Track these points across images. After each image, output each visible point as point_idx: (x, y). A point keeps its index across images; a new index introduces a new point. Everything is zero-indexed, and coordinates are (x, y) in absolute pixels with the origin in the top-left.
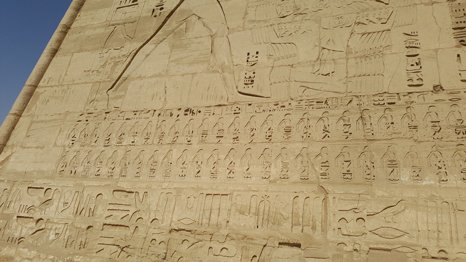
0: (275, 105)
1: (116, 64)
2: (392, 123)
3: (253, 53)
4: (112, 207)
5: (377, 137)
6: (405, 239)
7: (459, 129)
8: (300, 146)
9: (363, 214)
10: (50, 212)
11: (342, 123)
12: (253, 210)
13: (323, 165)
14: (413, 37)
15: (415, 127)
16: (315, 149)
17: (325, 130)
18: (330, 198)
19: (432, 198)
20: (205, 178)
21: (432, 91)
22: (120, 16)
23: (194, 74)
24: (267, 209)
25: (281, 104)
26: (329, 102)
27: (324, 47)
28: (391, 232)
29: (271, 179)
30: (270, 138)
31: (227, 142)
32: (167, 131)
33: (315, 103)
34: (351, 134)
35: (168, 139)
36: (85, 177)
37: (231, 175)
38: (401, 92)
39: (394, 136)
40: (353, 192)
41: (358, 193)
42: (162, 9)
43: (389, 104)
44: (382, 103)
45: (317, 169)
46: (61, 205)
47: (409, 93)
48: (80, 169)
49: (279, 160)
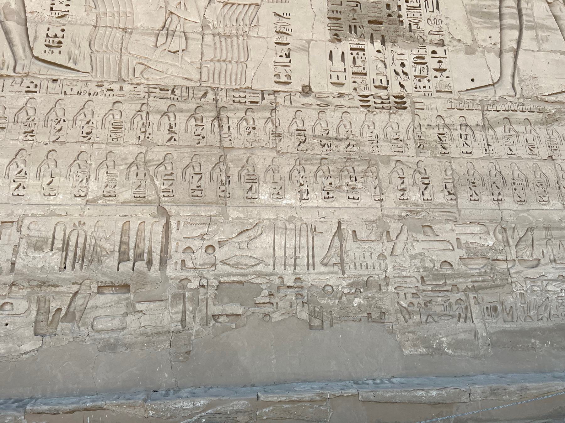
0: (98, 86)
2: (254, 128)
6: (260, 268)
7: (324, 141)
8: (135, 150)
11: (192, 122)
12: (58, 244)
13: (167, 177)
14: (284, 20)
15: (279, 135)
17: (170, 131)
21: (300, 92)
24: (81, 240)
25: (107, 86)
26: (178, 92)
29: (90, 197)
30: (89, 136)
33: (157, 90)
34: (203, 137)
37: (21, 191)
38: (267, 89)
40: (203, 214)
43: (251, 102)
44: (243, 100)
45: (157, 183)
47: (275, 92)
49: (103, 171)
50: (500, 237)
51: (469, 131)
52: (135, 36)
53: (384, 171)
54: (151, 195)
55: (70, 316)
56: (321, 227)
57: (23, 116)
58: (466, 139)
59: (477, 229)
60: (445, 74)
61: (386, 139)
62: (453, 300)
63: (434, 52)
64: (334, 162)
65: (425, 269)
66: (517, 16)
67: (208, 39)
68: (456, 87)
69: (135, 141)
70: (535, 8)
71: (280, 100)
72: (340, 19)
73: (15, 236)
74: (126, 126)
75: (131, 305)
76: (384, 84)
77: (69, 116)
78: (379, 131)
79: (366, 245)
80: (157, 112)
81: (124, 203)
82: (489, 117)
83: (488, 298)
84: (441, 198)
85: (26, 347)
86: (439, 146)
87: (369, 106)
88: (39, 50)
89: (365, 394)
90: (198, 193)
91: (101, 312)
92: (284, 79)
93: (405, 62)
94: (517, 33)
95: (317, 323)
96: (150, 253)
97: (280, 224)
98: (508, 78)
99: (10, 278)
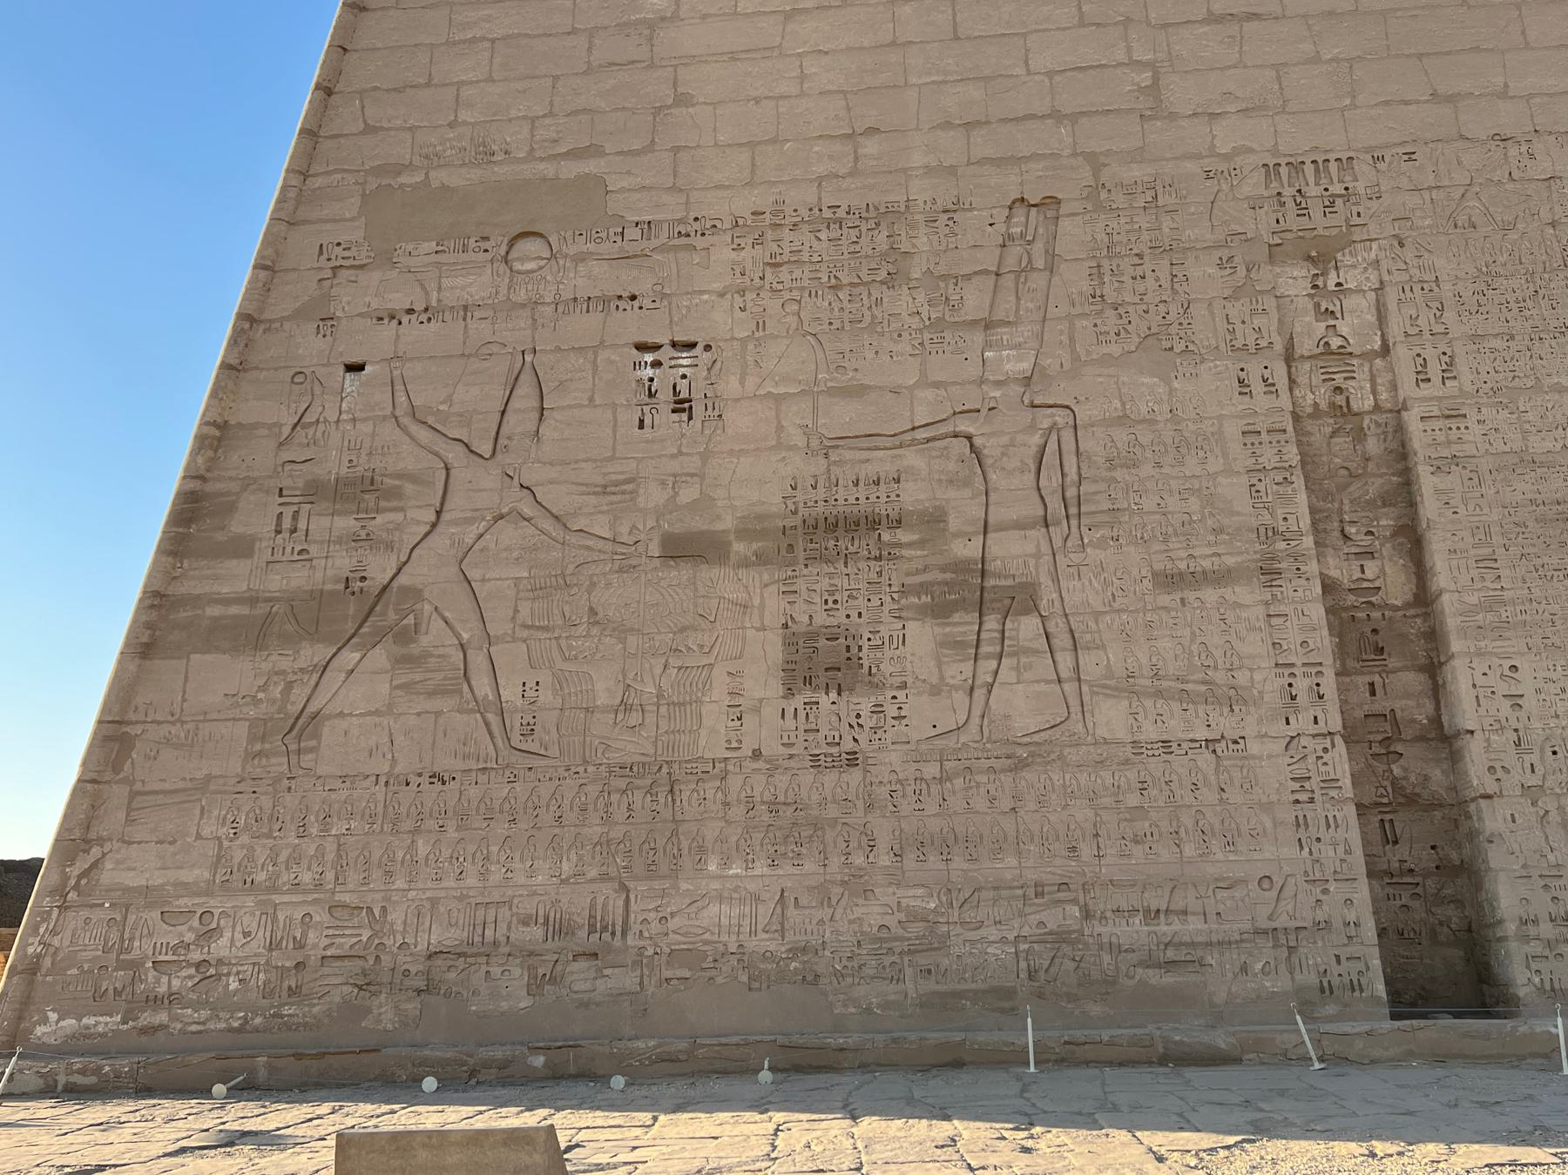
1: (289, 686)
3: (531, 684)
4: (331, 932)
6: (707, 936)
8: (599, 829)
10: (221, 947)
11: (649, 798)
12: (541, 920)
20: (471, 881)
22: (275, 583)
23: (438, 714)
25: (574, 769)
35: (408, 825)
36: (274, 889)
46: (239, 936)
48: (261, 877)
50: (944, 899)
51: (924, 786)
52: (598, 715)
53: (830, 835)
54: (613, 871)
55: (553, 980)
56: (765, 896)
57: (507, 806)
59: (920, 892)
60: (904, 722)
61: (834, 801)
62: (887, 964)
64: (780, 828)
65: (862, 933)
66: (998, 641)
67: (663, 709)
68: (915, 736)
69: (598, 821)
70: (1022, 627)
71: (730, 767)
73: (508, 914)
74: (591, 807)
75: (599, 970)
77: (543, 803)
78: (828, 793)
79: (807, 912)
80: (618, 791)
81: (592, 881)
83: (923, 960)
84: (885, 860)
85: (522, 1005)
88: (516, 740)
89: (781, 1040)
91: (576, 976)
92: (735, 745)
94: (994, 664)
95: (756, 985)
96: (613, 925)
97: (726, 894)
98: (975, 720)
99: (507, 950)
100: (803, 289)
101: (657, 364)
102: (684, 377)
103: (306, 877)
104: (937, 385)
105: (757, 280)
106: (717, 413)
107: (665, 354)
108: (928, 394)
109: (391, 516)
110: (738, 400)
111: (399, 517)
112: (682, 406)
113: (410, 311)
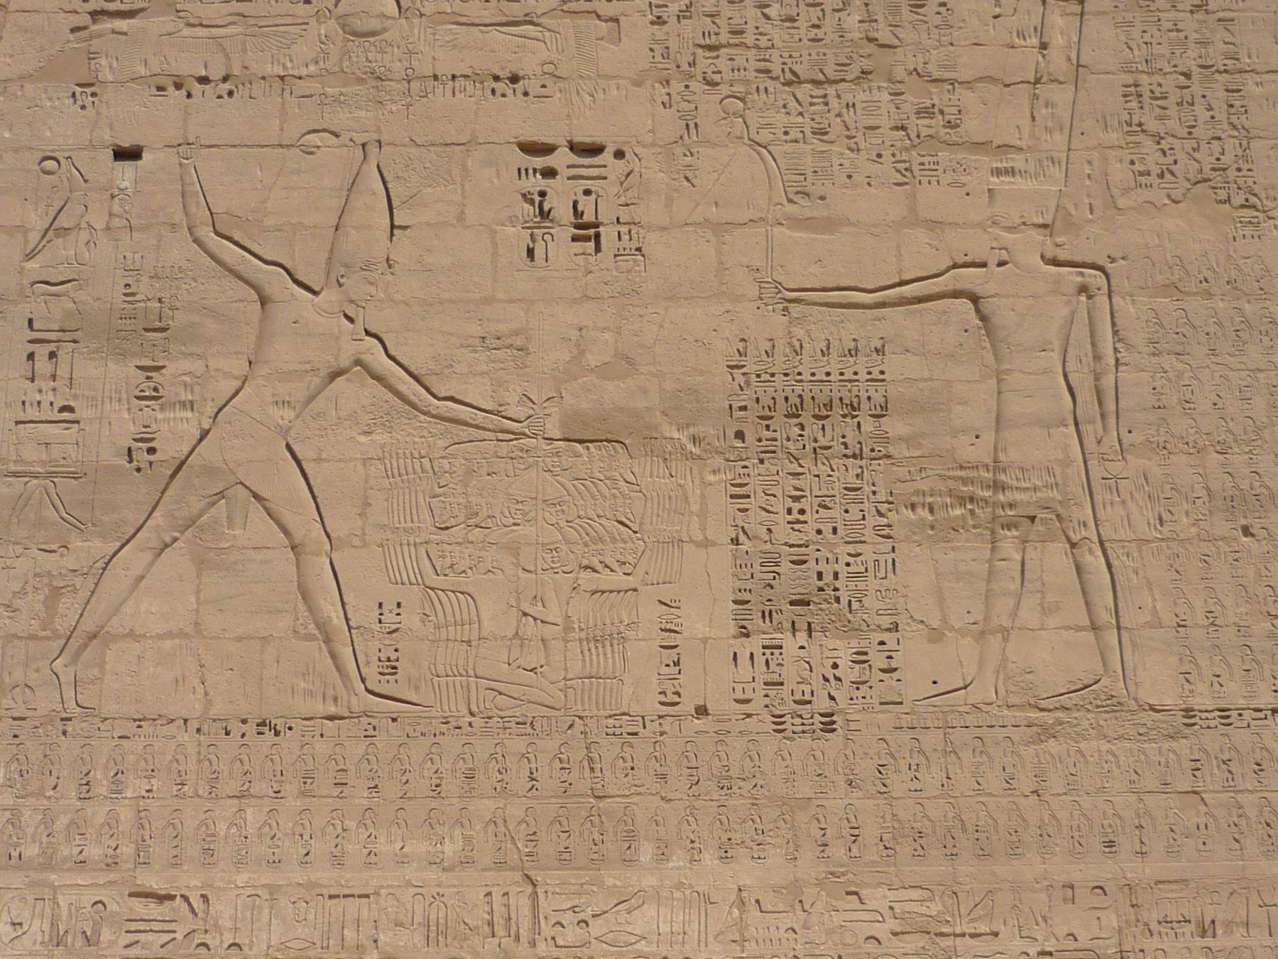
1: (56, 593)
5: (611, 790)
8: (490, 804)
9: (586, 915)
11: (557, 765)
12: (418, 919)
16: (516, 811)
18: (540, 891)
19: (680, 886)
23: (265, 640)
27: (527, 611)
28: (623, 938)
31: (360, 797)
32: (223, 767)
36: (48, 866)
37: (373, 858)
39: (634, 790)
41: (580, 881)
42: (151, 451)
44: (618, 731)
58: (917, 770)
59: (915, 894)
60: (895, 675)
63: (882, 643)
72: (748, 602)
76: (808, 697)
82: (952, 738)
86: (878, 782)
87: (784, 730)
90: (566, 856)
93: (838, 661)
100: (747, 82)
101: (550, 173)
102: (587, 192)
103: (94, 852)
104: (933, 225)
105: (685, 67)
106: (635, 244)
107: (561, 158)
108: (922, 236)
109: (186, 365)
110: (664, 229)
111: (198, 367)
112: (587, 231)
113: (204, 80)
